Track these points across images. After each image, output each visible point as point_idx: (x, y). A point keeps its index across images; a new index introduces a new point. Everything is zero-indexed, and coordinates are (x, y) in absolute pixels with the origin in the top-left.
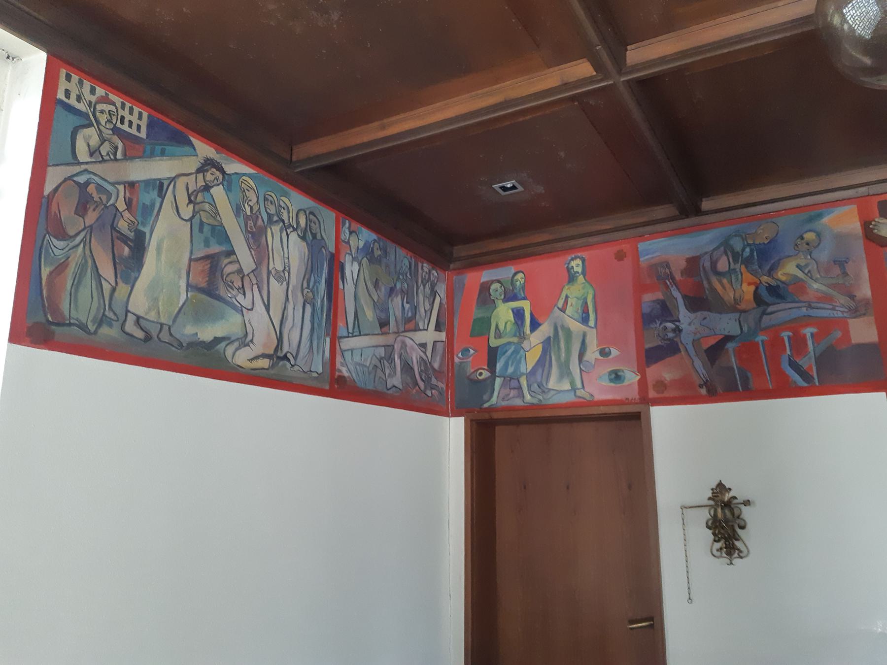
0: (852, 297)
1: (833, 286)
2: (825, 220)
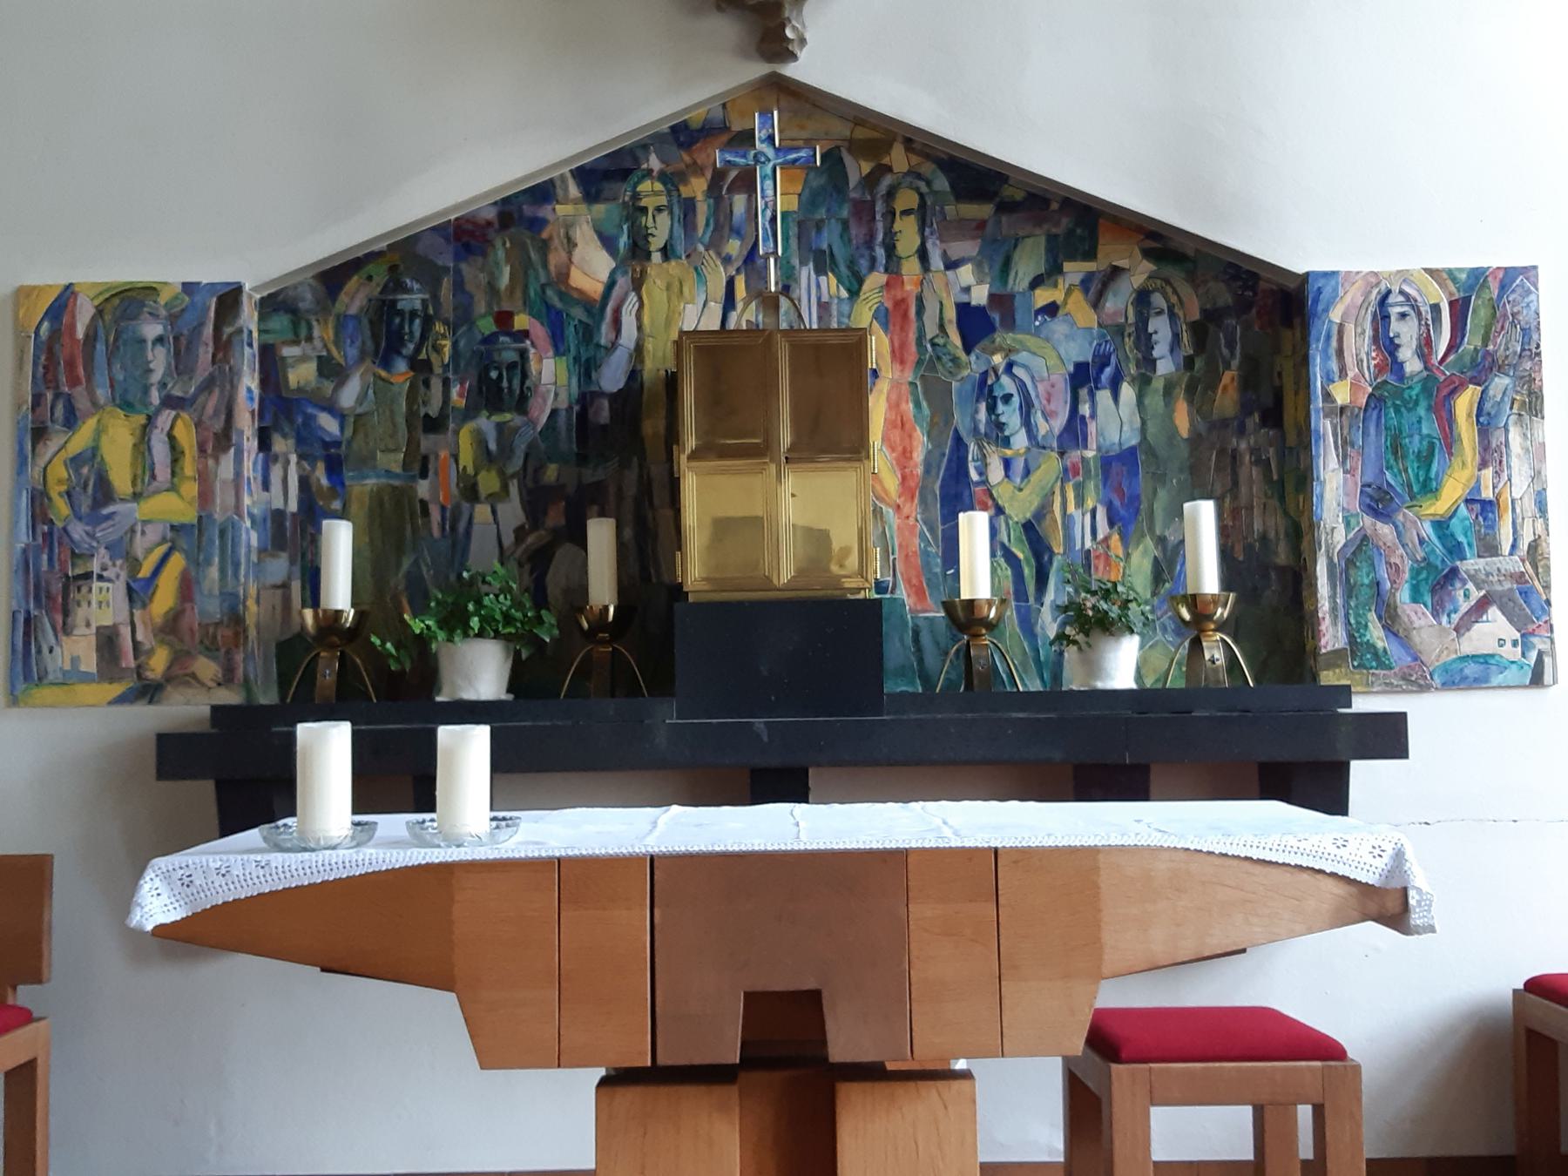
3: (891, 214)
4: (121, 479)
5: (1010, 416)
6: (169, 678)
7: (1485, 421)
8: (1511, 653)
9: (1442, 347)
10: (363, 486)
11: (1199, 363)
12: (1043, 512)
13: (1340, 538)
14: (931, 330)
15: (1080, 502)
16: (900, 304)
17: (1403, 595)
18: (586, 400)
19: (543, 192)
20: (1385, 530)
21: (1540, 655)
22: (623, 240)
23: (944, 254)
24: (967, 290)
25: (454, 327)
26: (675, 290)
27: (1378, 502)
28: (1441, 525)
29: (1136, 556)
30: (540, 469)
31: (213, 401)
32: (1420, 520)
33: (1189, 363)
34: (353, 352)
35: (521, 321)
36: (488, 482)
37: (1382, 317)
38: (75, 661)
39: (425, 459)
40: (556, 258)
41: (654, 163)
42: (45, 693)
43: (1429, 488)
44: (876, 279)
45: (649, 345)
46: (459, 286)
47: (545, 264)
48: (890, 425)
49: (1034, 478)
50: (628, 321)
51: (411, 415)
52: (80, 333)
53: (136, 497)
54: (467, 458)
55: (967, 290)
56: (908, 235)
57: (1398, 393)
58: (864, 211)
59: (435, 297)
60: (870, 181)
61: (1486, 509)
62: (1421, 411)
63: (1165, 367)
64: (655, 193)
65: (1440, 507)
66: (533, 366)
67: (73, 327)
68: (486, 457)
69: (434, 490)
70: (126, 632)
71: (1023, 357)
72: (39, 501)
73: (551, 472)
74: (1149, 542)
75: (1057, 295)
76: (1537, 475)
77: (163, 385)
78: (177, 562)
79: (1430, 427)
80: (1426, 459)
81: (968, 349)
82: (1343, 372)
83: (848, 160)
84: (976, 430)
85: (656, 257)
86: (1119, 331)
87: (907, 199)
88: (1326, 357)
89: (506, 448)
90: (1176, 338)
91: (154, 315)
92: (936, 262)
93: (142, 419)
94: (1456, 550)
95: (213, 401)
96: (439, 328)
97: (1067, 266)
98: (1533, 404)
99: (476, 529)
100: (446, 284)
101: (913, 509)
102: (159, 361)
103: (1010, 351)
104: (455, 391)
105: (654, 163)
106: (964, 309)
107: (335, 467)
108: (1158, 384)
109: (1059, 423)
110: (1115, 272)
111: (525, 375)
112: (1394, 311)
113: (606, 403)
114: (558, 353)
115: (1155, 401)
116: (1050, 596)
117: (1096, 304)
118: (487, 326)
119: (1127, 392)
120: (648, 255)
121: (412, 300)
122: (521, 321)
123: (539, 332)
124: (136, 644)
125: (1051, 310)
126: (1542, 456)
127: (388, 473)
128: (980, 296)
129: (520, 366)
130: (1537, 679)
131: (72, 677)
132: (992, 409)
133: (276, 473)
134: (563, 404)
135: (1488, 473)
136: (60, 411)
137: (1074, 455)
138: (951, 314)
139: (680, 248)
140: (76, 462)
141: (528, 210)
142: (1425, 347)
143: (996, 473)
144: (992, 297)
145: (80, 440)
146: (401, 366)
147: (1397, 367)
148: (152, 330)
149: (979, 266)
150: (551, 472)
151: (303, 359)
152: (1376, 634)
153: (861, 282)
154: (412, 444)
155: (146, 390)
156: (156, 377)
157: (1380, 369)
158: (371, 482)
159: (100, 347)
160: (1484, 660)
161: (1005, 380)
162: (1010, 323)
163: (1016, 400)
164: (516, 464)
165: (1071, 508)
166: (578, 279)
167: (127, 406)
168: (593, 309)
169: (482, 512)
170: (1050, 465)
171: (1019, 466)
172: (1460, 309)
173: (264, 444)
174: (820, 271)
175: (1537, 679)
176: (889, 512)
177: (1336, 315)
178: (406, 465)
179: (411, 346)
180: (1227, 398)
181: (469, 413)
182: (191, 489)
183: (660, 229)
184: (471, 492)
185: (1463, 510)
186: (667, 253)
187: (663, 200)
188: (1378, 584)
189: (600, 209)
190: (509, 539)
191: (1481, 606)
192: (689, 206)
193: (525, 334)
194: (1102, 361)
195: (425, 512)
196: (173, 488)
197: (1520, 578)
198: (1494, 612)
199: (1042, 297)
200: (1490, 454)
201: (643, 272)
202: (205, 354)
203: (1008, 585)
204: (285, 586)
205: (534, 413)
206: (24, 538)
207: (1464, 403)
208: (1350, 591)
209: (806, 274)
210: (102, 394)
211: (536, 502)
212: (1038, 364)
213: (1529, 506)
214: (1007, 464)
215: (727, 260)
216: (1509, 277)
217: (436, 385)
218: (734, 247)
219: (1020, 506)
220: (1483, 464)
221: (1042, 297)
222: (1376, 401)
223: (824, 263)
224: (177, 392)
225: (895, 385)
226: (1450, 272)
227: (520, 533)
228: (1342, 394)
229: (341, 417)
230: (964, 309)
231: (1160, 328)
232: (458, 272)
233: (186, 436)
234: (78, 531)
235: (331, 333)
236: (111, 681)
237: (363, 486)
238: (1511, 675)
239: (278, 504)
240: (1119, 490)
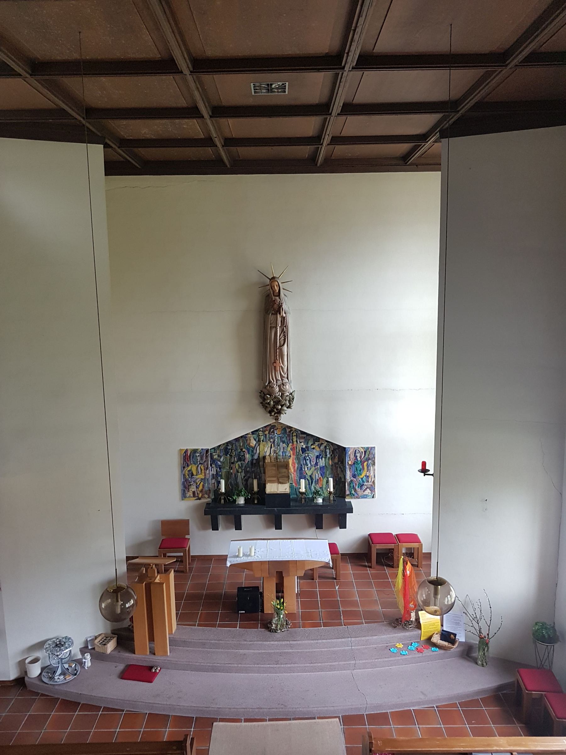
3: (292, 436)
4: (195, 473)
5: (308, 462)
6: (202, 497)
7: (368, 466)
8: (370, 494)
10: (224, 471)
11: (333, 455)
12: (312, 474)
14: (298, 451)
15: (317, 473)
16: (294, 448)
17: (357, 487)
18: (252, 460)
20: (355, 479)
21: (374, 495)
22: (257, 439)
23: (300, 441)
24: (303, 446)
25: (235, 451)
26: (264, 446)
28: (362, 479)
29: (324, 480)
30: (247, 469)
31: (206, 463)
33: (331, 455)
34: (222, 454)
35: (244, 450)
36: (240, 470)
37: (355, 453)
38: (190, 495)
39: (232, 467)
42: (187, 499)
43: (361, 474)
44: (291, 444)
45: (261, 453)
46: (236, 446)
47: (247, 442)
48: (292, 463)
49: (311, 470)
51: (230, 462)
52: (189, 455)
53: (196, 475)
54: (237, 467)
55: (303, 446)
57: (357, 463)
58: (289, 436)
59: (233, 447)
60: (290, 432)
61: (367, 477)
62: (360, 465)
63: (328, 456)
64: (261, 433)
65: (362, 477)
66: (246, 456)
67: (188, 454)
69: (233, 471)
70: (196, 491)
71: (310, 454)
72: (184, 475)
73: (248, 469)
74: (326, 478)
75: (315, 447)
76: (374, 473)
77: (199, 461)
78: (202, 483)
79: (361, 467)
80: (360, 471)
81: (303, 453)
82: (350, 460)
83: (287, 429)
84: (304, 464)
85: (262, 442)
86: (322, 451)
87: (295, 434)
88: (348, 458)
89: (242, 466)
90: (330, 452)
91: (198, 453)
92: (299, 442)
93: (197, 466)
94: (363, 482)
95: (206, 463)
96: (233, 451)
97: (316, 443)
98: (374, 464)
99: (239, 476)
100: (234, 445)
101: (295, 473)
102: (199, 458)
103: (308, 454)
104: (235, 459)
105: (261, 429)
106: (302, 448)
107: (220, 469)
108: (327, 458)
109: (314, 463)
110: (322, 444)
111: (244, 457)
112: (357, 452)
113: (255, 460)
114: (249, 453)
115: (327, 460)
116: (313, 485)
118: (239, 450)
119: (323, 459)
120: (260, 441)
121: (229, 448)
122: (244, 450)
123: (246, 451)
124: (197, 493)
125: (314, 448)
126: (375, 471)
127: (227, 469)
128: (304, 447)
129: (244, 455)
130: (373, 497)
131: (190, 497)
132: (306, 461)
133: (213, 469)
134: (249, 460)
135: (368, 472)
136: (186, 465)
137: (316, 467)
138: (300, 449)
139: (265, 440)
140: (189, 471)
142: (360, 457)
143: (306, 469)
144: (306, 446)
145: (189, 468)
147: (357, 459)
148: (198, 455)
149: (304, 442)
150: (248, 469)
151: (216, 455)
153: (289, 445)
154: (230, 465)
155: (197, 462)
156: (198, 461)
157: (355, 459)
158: (225, 470)
159: (191, 457)
161: (307, 457)
162: (308, 450)
163: (309, 460)
164: (244, 468)
165: (316, 474)
166: (251, 444)
167: (195, 464)
168: (253, 448)
169: (239, 474)
171: (309, 468)
172: (365, 452)
173: (211, 466)
174: (283, 443)
175: (373, 497)
176: (292, 474)
177: (349, 453)
178: (229, 468)
179: (230, 453)
180: (336, 461)
181: (237, 462)
182: (203, 474)
183: (262, 438)
184: (238, 472)
185: (365, 477)
186: (263, 441)
187: (262, 434)
188: (353, 486)
189: (254, 435)
190: (243, 478)
191: (367, 488)
192: (266, 435)
193: (244, 451)
195: (232, 474)
196: (201, 474)
197: (371, 485)
198: (368, 489)
199: (312, 447)
200: (368, 470)
201: (260, 444)
202: (205, 457)
203: (308, 483)
204: (214, 483)
205: (246, 461)
206: (183, 480)
207: (365, 464)
208: (350, 487)
209: (281, 443)
210: (192, 463)
211: (246, 472)
212: (312, 455)
213: (373, 476)
214: (308, 468)
215: (271, 442)
216: (372, 448)
217: (233, 458)
218: (272, 440)
219: (309, 473)
220: (367, 471)
221: (312, 447)
222: (354, 463)
223: (284, 442)
224: (201, 462)
225: (293, 458)
226: (364, 448)
227: (244, 477)
228: (350, 463)
229: (221, 462)
230: (302, 448)
232: (236, 443)
233: (202, 468)
234: (189, 479)
235: (219, 451)
236: (195, 497)
237: (224, 471)
238: (370, 497)
239: (213, 473)
240: (322, 471)
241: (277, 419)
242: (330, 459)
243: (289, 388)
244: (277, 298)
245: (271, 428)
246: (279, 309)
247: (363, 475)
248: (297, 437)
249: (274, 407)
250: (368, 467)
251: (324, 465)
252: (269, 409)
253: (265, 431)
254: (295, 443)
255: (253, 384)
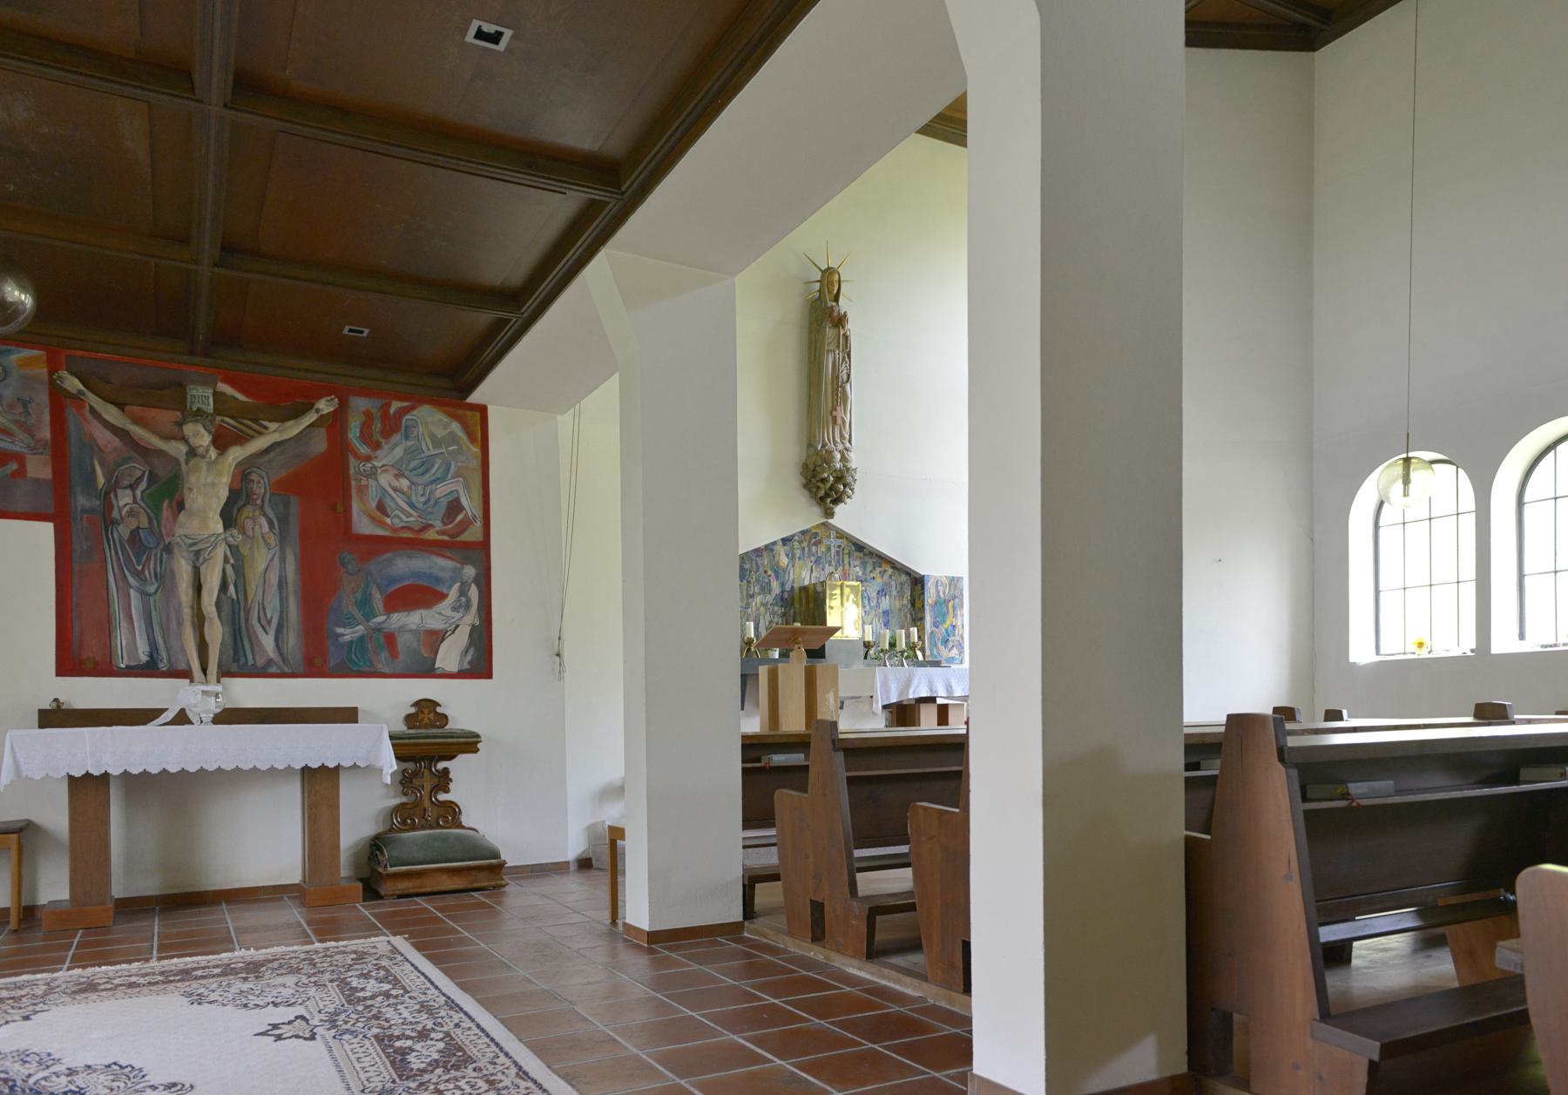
0: (32, 436)
1: (16, 422)
2: (14, 357)
3: (843, 554)
7: (954, 608)
8: (957, 657)
9: (947, 592)
13: (930, 631)
17: (939, 644)
18: (783, 592)
19: (774, 543)
20: (937, 630)
26: (801, 569)
27: (936, 624)
32: (943, 628)
35: (770, 572)
37: (937, 586)
40: (776, 559)
41: (796, 538)
43: (944, 622)
46: (757, 564)
50: (791, 574)
56: (846, 557)
61: (954, 627)
65: (946, 626)
68: (762, 604)
76: (962, 620)
79: (945, 609)
80: (944, 616)
100: (754, 562)
115: (892, 601)
117: (882, 577)
139: (802, 557)
141: (771, 547)
146: (745, 582)
152: (935, 652)
160: (953, 658)
166: (781, 564)
170: (873, 613)
181: (759, 594)
183: (798, 553)
189: (786, 547)
192: (804, 549)
193: (770, 576)
194: (883, 590)
199: (872, 575)
200: (955, 616)
207: (950, 605)
208: (931, 643)
213: (961, 627)
217: (752, 586)
218: (813, 559)
221: (872, 575)
222: (936, 603)
231: (893, 583)
241: (829, 513)
242: (897, 599)
243: (855, 460)
244: (834, 304)
245: (810, 537)
246: (840, 321)
247: (948, 623)
248: (849, 557)
249: (832, 488)
250: (954, 611)
251: (888, 608)
252: (822, 493)
253: (802, 542)
254: (847, 567)
255: (792, 454)
